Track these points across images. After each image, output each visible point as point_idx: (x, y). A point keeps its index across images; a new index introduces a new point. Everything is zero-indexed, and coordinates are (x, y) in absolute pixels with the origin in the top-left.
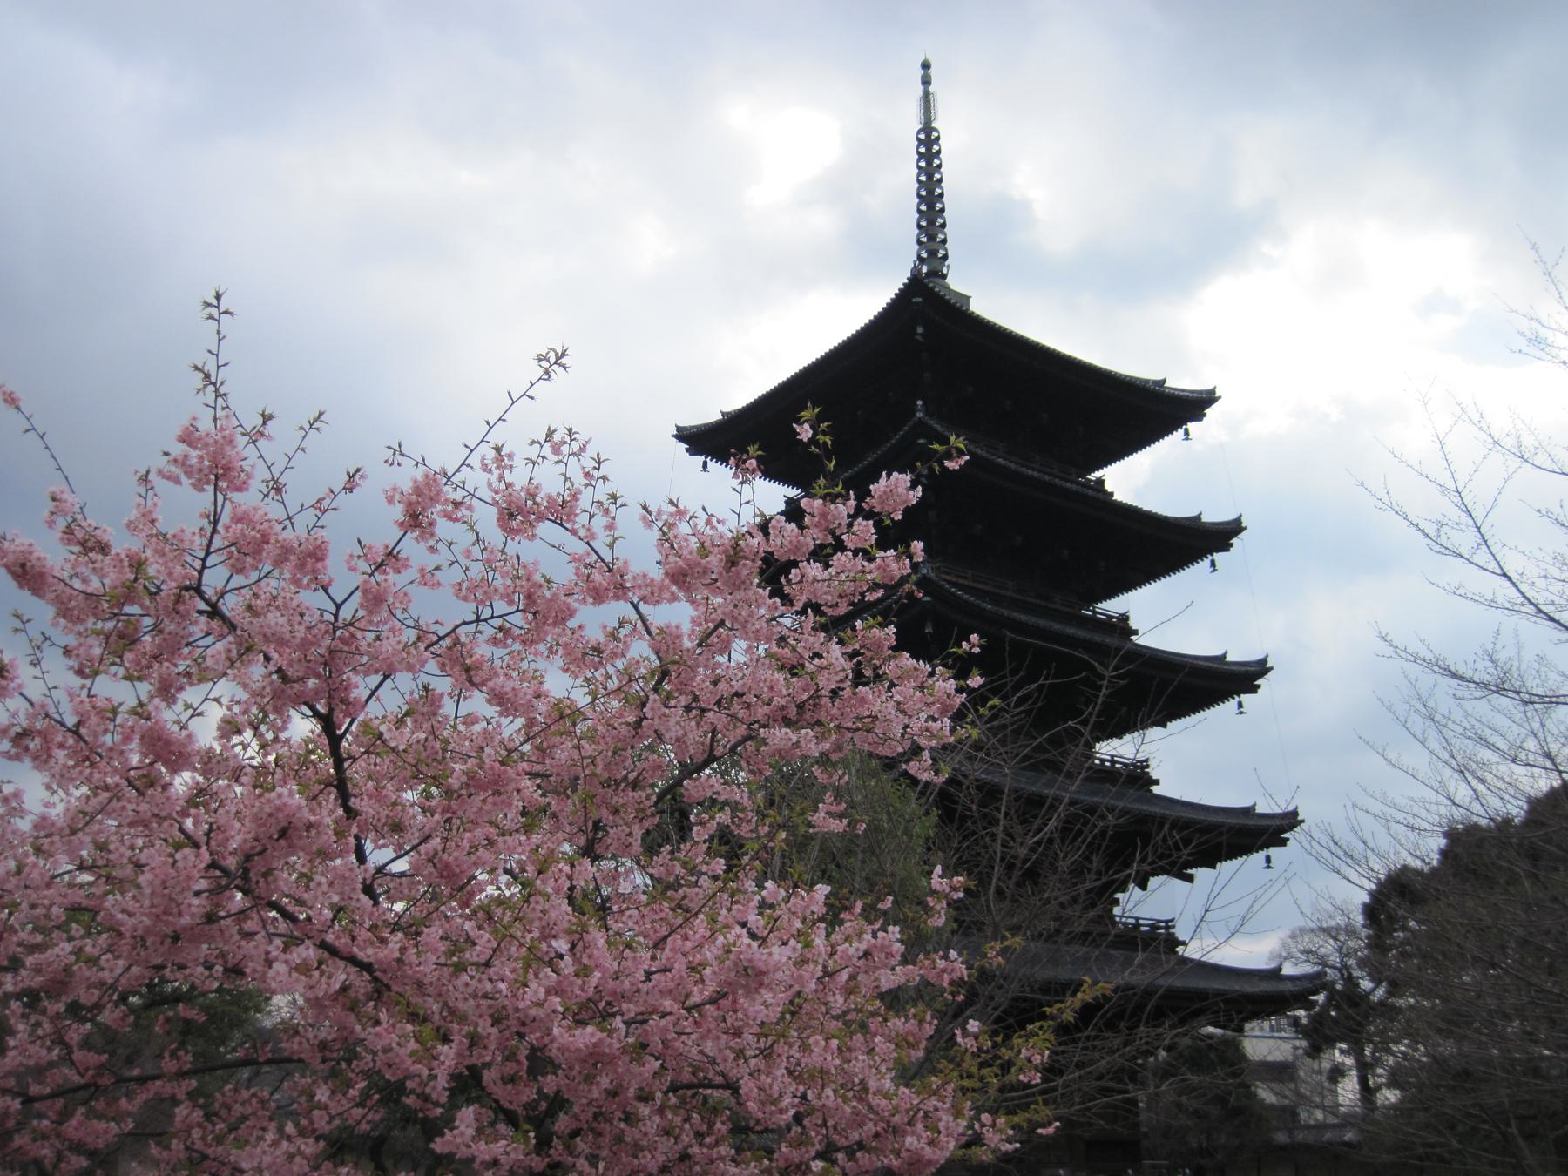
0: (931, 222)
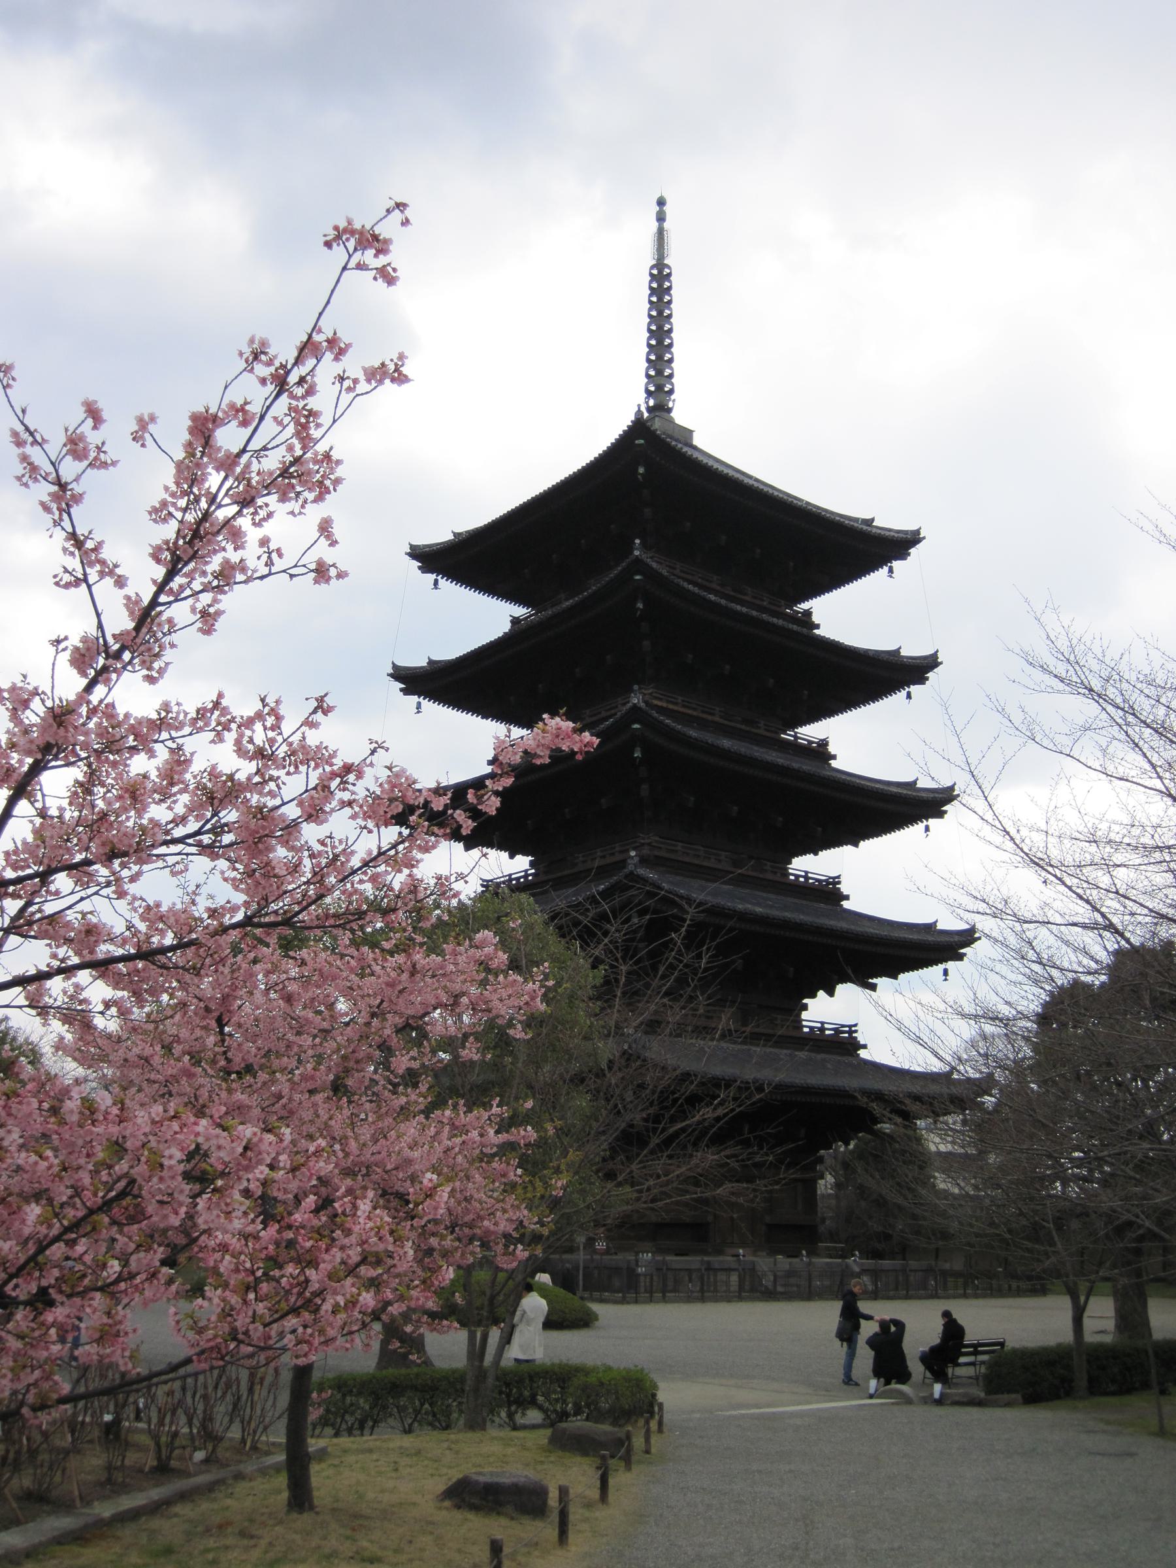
0: (660, 358)
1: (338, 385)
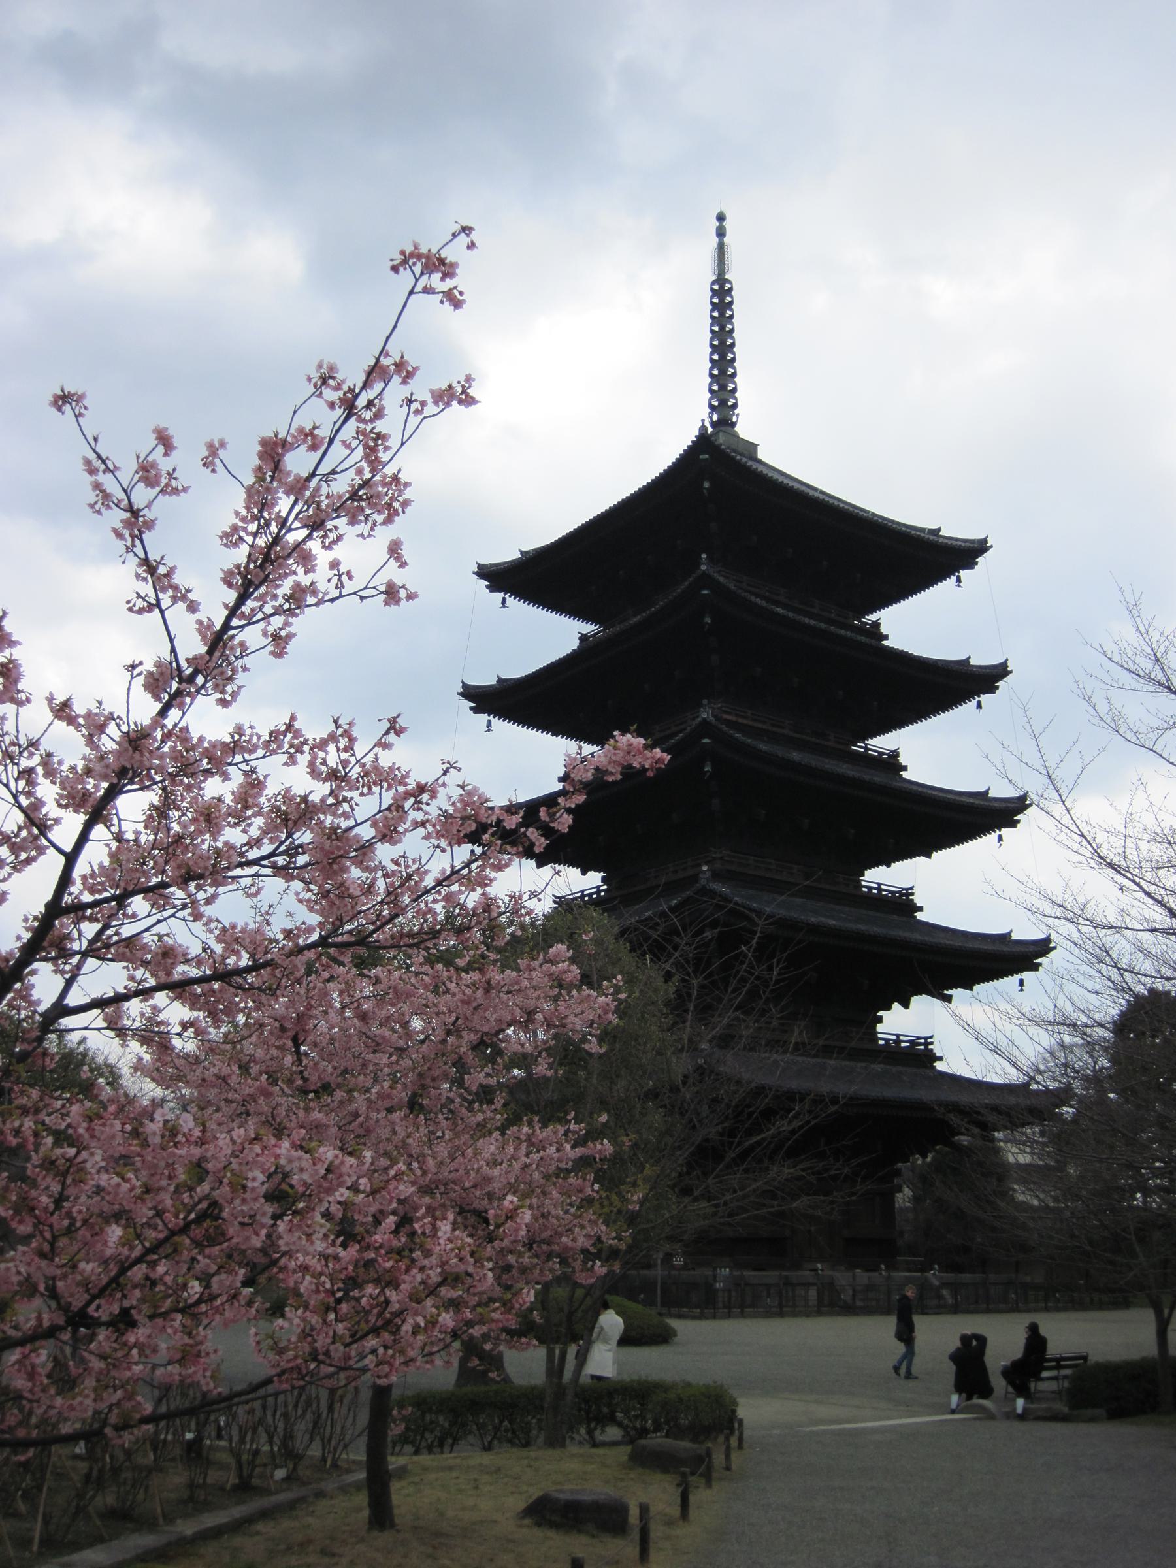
0: (723, 372)
1: (406, 408)
